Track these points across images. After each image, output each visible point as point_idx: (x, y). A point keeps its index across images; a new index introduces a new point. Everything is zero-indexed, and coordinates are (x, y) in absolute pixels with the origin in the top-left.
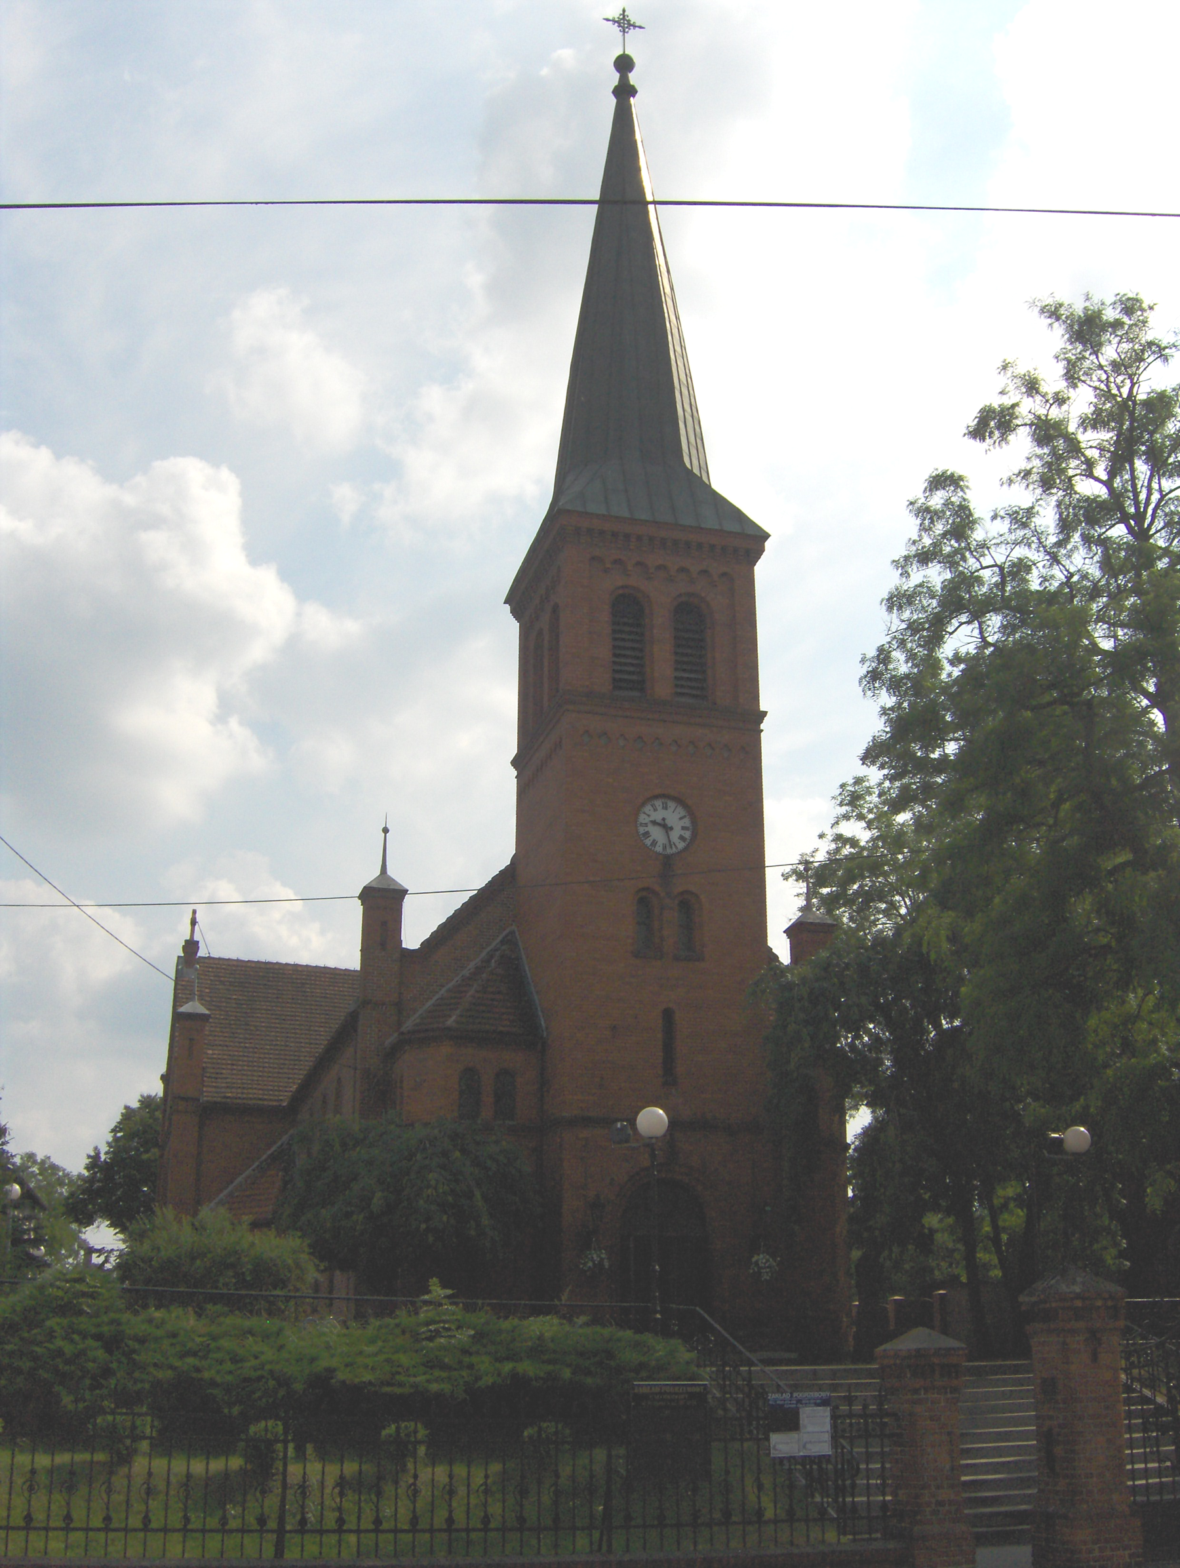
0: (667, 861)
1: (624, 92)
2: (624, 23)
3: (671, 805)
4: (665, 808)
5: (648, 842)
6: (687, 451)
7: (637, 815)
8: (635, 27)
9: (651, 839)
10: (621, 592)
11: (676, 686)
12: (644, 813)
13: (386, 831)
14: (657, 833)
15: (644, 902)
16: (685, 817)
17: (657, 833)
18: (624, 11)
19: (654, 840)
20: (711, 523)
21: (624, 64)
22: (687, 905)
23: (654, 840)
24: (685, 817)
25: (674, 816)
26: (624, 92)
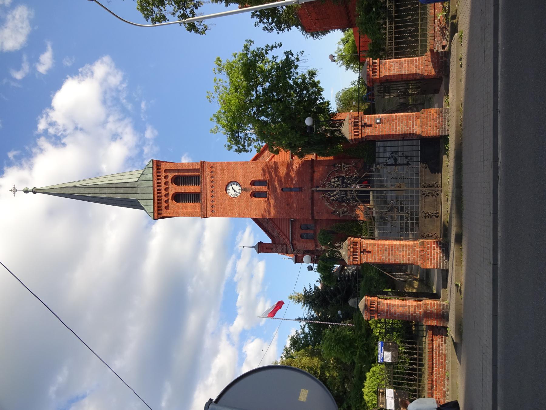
0: (243, 190)
1: (35, 191)
2: (14, 190)
6: (133, 179)
8: (14, 188)
13: (244, 247)
15: (254, 195)
18: (10, 190)
21: (26, 191)
22: (253, 183)
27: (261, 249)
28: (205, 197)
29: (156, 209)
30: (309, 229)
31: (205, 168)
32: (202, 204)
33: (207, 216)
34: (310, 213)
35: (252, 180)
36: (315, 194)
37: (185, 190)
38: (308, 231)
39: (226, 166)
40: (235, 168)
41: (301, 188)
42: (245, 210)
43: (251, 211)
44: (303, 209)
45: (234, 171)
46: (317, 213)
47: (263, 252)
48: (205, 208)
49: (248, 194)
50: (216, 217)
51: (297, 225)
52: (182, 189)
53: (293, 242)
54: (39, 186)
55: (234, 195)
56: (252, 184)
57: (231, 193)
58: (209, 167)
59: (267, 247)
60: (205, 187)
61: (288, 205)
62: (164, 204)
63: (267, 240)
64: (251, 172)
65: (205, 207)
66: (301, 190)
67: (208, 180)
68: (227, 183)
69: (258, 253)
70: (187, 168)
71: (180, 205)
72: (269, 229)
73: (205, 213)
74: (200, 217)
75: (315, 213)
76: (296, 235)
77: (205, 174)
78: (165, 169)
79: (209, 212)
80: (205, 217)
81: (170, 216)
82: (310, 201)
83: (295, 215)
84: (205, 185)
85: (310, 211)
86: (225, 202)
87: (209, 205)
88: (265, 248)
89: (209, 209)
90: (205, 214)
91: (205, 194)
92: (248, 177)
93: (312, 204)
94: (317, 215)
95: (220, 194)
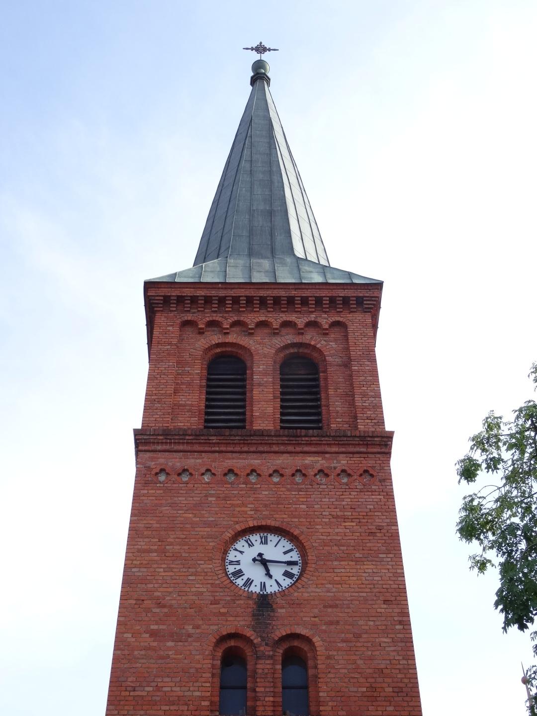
0: (264, 602)
1: (259, 77)
3: (273, 538)
4: (265, 542)
5: (240, 582)
7: (225, 552)
9: (245, 578)
10: (218, 350)
11: (282, 428)
12: (236, 550)
14: (256, 574)
16: (291, 550)
17: (256, 574)
19: (240, 571)
20: (317, 278)
23: (240, 571)
24: (291, 550)
26: (259, 77)
29: (188, 292)
32: (197, 435)
33: (141, 454)
37: (259, 385)
39: (380, 528)
40: (369, 567)
42: (160, 605)
43: (154, 634)
45: (357, 561)
48: (181, 447)
49: (241, 623)
50: (136, 488)
52: (265, 374)
54: (275, 92)
55: (238, 563)
56: (296, 643)
60: (275, 448)
62: (202, 318)
64: (358, 636)
65: (185, 447)
67: (309, 460)
68: (296, 532)
71: (197, 371)
73: (159, 447)
74: (139, 427)
77: (335, 449)
78: (349, 324)
79: (162, 461)
80: (140, 448)
81: (156, 332)
84: (282, 448)
87: (192, 462)
89: (176, 462)
90: (153, 447)
91: (246, 449)
92: (331, 623)
95: (244, 505)
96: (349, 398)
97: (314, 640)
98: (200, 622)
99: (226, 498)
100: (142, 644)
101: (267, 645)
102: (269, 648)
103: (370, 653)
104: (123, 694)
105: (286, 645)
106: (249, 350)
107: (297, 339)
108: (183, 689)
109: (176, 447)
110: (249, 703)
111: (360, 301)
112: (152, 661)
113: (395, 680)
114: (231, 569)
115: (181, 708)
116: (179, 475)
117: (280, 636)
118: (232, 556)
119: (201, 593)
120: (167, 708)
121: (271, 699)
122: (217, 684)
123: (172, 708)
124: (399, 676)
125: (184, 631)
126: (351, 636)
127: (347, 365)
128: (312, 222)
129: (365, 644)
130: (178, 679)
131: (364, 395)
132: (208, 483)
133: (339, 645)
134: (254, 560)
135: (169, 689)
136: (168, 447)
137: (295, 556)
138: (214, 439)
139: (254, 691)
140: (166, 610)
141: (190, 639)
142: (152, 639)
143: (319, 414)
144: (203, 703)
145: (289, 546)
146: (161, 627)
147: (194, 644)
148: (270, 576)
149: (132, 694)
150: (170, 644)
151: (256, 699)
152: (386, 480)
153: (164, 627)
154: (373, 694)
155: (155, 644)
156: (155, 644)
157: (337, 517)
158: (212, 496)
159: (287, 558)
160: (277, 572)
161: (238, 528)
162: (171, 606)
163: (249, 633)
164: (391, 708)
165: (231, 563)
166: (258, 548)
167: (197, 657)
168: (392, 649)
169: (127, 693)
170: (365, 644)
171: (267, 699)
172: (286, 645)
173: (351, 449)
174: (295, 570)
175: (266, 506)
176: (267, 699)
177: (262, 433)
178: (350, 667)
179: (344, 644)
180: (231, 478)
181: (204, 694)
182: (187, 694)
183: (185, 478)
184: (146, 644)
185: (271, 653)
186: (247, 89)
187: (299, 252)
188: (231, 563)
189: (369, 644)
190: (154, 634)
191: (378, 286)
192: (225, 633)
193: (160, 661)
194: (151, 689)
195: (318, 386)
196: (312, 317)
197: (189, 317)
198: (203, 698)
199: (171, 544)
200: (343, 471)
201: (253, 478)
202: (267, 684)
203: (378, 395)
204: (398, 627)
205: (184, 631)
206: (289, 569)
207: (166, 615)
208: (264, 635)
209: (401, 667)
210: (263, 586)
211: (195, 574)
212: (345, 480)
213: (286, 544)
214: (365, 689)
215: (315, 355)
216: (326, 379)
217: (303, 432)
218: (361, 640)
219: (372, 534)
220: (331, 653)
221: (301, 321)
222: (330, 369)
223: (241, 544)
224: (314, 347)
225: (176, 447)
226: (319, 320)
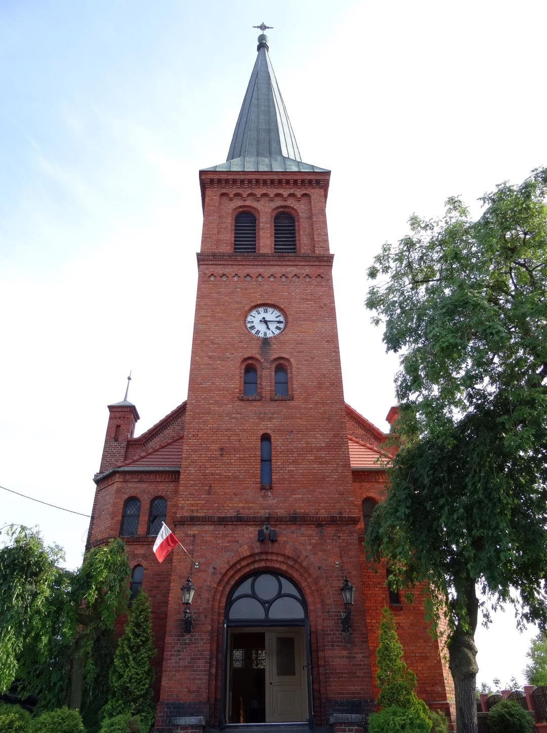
0: (266, 341)
1: (262, 46)
3: (270, 310)
4: (266, 312)
5: (253, 332)
7: (246, 317)
9: (256, 330)
10: (241, 210)
12: (251, 316)
13: (129, 379)
16: (280, 316)
17: (262, 328)
19: (254, 326)
20: (295, 169)
22: (281, 366)
23: (254, 326)
24: (280, 316)
25: (272, 315)
26: (262, 46)
27: (118, 415)
28: (247, 263)
29: (223, 177)
30: (153, 522)
31: (318, 264)
33: (200, 266)
34: (195, 514)
35: (292, 360)
36: (251, 529)
37: (263, 229)
38: (147, 519)
39: (325, 305)
40: (320, 324)
41: (271, 488)
43: (210, 357)
44: (209, 493)
45: (313, 321)
46: (194, 536)
47: (111, 418)
48: (222, 263)
49: (254, 352)
50: (199, 284)
51: (165, 488)
53: (117, 475)
54: (272, 56)
55: (252, 322)
56: (282, 362)
57: (255, 318)
58: (320, 271)
59: (122, 427)
60: (271, 263)
61: (222, 449)
62: (232, 191)
63: (140, 429)
64: (313, 358)
65: (224, 263)
66: (266, 486)
67: (289, 269)
69: (111, 408)
70: (315, 232)
71: (229, 221)
72: (166, 432)
73: (210, 263)
74: (199, 252)
75: (194, 530)
76: (139, 485)
77: (303, 263)
78: (312, 195)
79: (212, 270)
80: (200, 263)
81: (206, 200)
82: (231, 513)
83: (192, 470)
84: (275, 263)
85: (199, 515)
86: (237, 303)
87: (228, 270)
88: (120, 422)
89: (219, 270)
90: (207, 263)
91: (256, 263)
92: (300, 352)
93: (223, 521)
94: (187, 536)
95: (255, 293)
96: (311, 236)
97: (291, 360)
98: (234, 352)
99: (246, 289)
100: (205, 362)
101: (267, 362)
102: (268, 364)
103: (318, 366)
104: (196, 386)
105: (277, 363)
106: (257, 210)
107: (283, 204)
108: (226, 383)
109: (219, 263)
110: (258, 391)
111: (318, 182)
112: (210, 370)
113: (331, 379)
114: (249, 325)
115: (225, 392)
116: (221, 277)
117: (274, 358)
118: (249, 319)
119: (234, 337)
120: (218, 392)
121: (269, 388)
122: (243, 381)
123: (220, 392)
124: (333, 377)
125: (225, 356)
126: (310, 358)
127: (310, 218)
128: (293, 136)
129: (317, 362)
130: (223, 379)
131: (319, 234)
132: (237, 282)
133: (304, 362)
134: (261, 321)
135: (219, 384)
136: (215, 262)
137: (281, 319)
138: (239, 258)
139: (261, 384)
140: (216, 345)
141: (228, 360)
142: (209, 360)
143: (295, 245)
144: (236, 390)
145: (278, 314)
146: (214, 354)
147: (231, 362)
148: (268, 328)
149: (201, 386)
150: (218, 362)
151: (262, 388)
152: (329, 280)
153: (215, 354)
154: (320, 386)
155: (211, 362)
156: (211, 362)
157: (304, 299)
158: (238, 288)
159: (278, 319)
160: (273, 326)
161: (253, 304)
162: (218, 344)
163: (258, 356)
164: (329, 393)
165: (249, 322)
166: (263, 315)
167: (232, 368)
168: (330, 364)
169: (198, 386)
170: (317, 362)
171: (267, 388)
172: (277, 363)
173: (312, 263)
174: (282, 326)
175: (267, 293)
176: (267, 388)
177: (264, 255)
178: (309, 373)
179: (306, 362)
180: (248, 279)
181: (236, 386)
182: (227, 386)
183: (224, 279)
184: (207, 362)
185: (269, 366)
186: (256, 53)
187: (285, 154)
188: (249, 322)
189: (319, 362)
190: (210, 357)
191: (328, 173)
192: (246, 357)
193: (214, 370)
194: (209, 384)
195: (294, 230)
196: (292, 191)
197: (224, 191)
198: (235, 388)
199: (218, 313)
200: (307, 275)
201: (260, 279)
202: (268, 381)
203: (326, 235)
204: (333, 354)
205: (225, 356)
206: (278, 325)
207: (216, 348)
208: (266, 358)
209: (334, 373)
210: (265, 334)
211: (231, 328)
212: (308, 280)
213: (277, 313)
214: (316, 384)
215: (293, 212)
216: (299, 226)
217: (287, 254)
218: (315, 360)
219: (322, 307)
220: (299, 366)
221: (285, 193)
222: (301, 220)
223: (254, 313)
224: (293, 208)
225: (219, 263)
226: (295, 193)
